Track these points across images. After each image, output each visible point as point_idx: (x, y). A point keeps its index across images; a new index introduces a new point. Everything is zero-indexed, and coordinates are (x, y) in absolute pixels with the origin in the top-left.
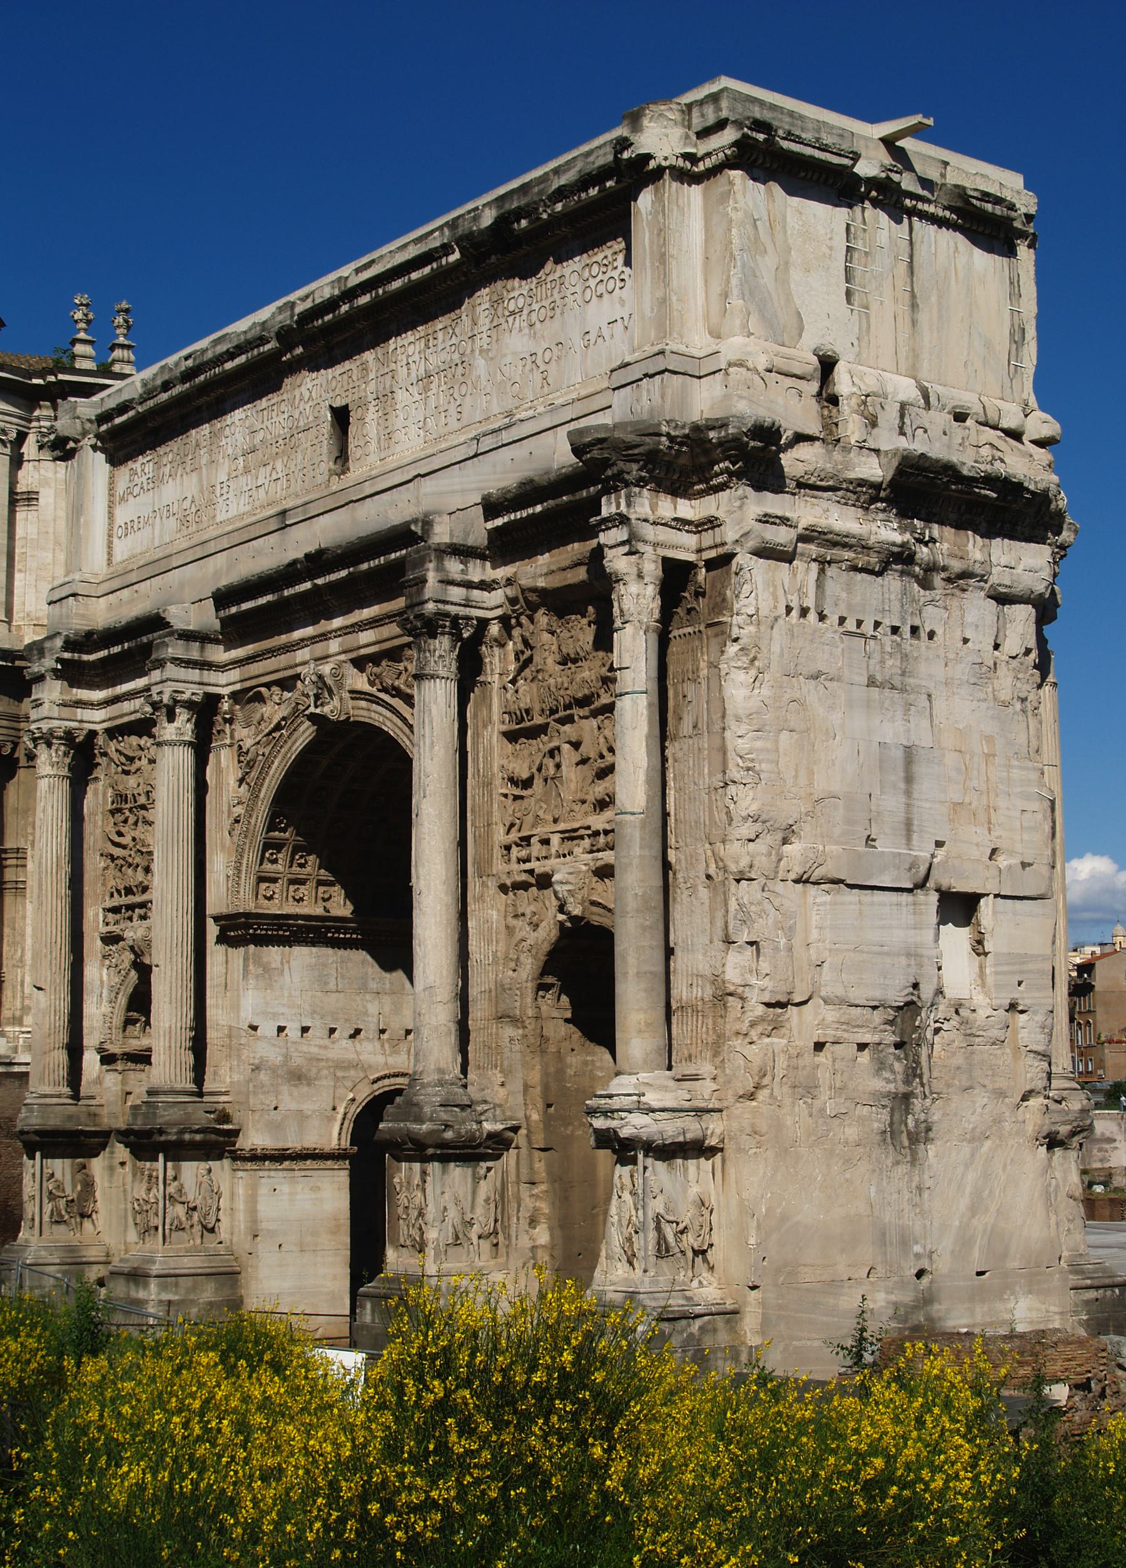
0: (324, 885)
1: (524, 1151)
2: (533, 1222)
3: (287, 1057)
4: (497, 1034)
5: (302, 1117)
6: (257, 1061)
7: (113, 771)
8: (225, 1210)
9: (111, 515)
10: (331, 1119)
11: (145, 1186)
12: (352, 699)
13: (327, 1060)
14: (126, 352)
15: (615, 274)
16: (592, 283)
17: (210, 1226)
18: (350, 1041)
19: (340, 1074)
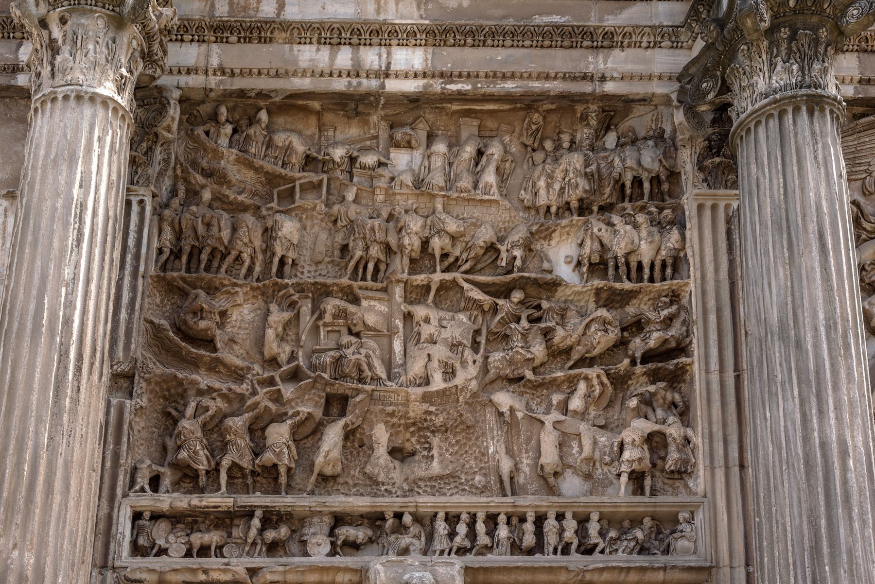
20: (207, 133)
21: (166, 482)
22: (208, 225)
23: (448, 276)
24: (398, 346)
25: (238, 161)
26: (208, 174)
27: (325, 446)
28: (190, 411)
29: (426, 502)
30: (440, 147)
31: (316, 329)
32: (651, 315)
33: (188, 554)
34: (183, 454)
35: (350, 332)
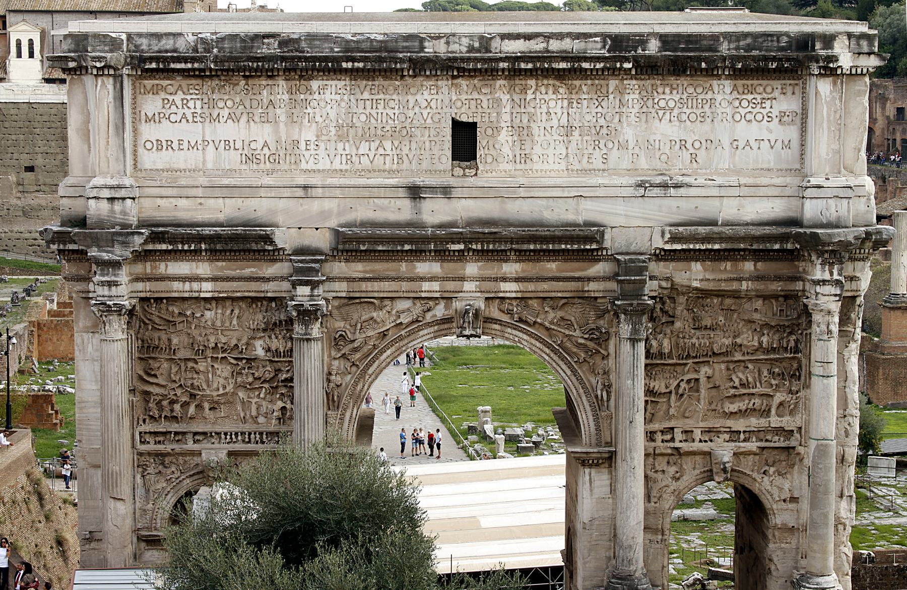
9: (135, 131)
15: (764, 112)
16: (743, 112)
20: (148, 306)
21: (147, 421)
22: (151, 340)
23: (223, 355)
24: (210, 376)
25: (158, 316)
26: (149, 320)
27: (190, 413)
28: (152, 401)
29: (218, 430)
30: (220, 311)
31: (186, 371)
32: (283, 369)
33: (155, 444)
34: (151, 414)
35: (196, 373)
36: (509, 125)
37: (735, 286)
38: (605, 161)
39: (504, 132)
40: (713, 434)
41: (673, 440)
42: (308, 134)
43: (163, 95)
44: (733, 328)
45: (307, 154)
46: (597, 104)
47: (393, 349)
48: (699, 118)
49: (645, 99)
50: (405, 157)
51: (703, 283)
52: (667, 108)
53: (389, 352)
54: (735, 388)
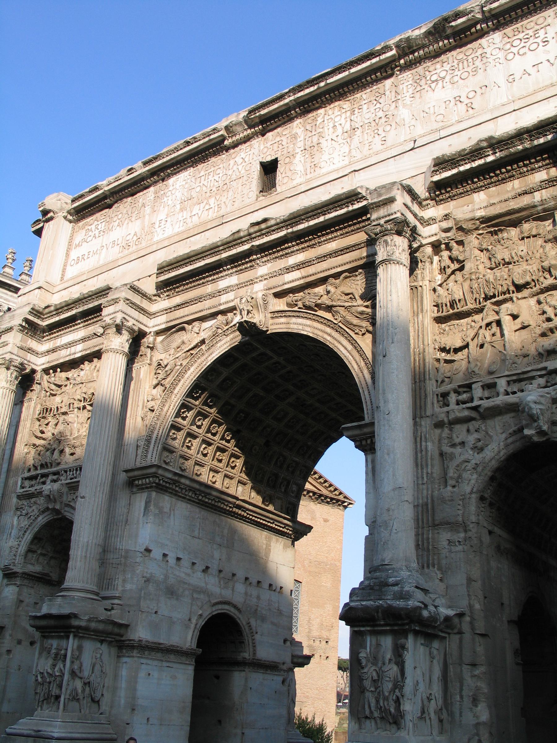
0: (198, 465)
1: (467, 636)
2: (475, 701)
3: (166, 577)
4: (433, 539)
5: (171, 622)
6: (148, 576)
7: (43, 395)
8: (108, 687)
9: (67, 255)
10: (187, 627)
11: (50, 662)
12: (272, 318)
13: (189, 584)
14: (27, 277)
17: (97, 699)
18: (203, 574)
19: (195, 596)
36: (303, 148)
37: (526, 201)
38: (384, 142)
39: (299, 157)
40: (523, 383)
41: (472, 400)
42: (162, 216)
43: (87, 227)
44: (538, 255)
45: (158, 230)
46: (375, 102)
47: (196, 365)
48: (471, 74)
49: (418, 81)
50: (223, 205)
51: (488, 209)
52: (439, 79)
53: (192, 369)
54: (549, 320)
